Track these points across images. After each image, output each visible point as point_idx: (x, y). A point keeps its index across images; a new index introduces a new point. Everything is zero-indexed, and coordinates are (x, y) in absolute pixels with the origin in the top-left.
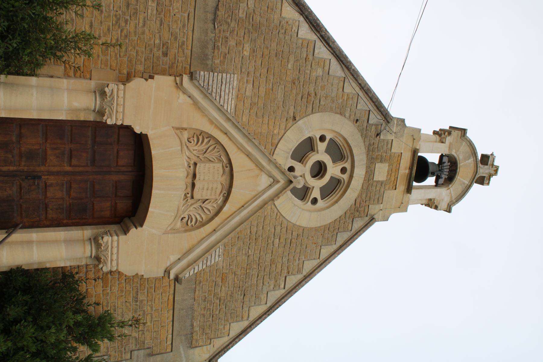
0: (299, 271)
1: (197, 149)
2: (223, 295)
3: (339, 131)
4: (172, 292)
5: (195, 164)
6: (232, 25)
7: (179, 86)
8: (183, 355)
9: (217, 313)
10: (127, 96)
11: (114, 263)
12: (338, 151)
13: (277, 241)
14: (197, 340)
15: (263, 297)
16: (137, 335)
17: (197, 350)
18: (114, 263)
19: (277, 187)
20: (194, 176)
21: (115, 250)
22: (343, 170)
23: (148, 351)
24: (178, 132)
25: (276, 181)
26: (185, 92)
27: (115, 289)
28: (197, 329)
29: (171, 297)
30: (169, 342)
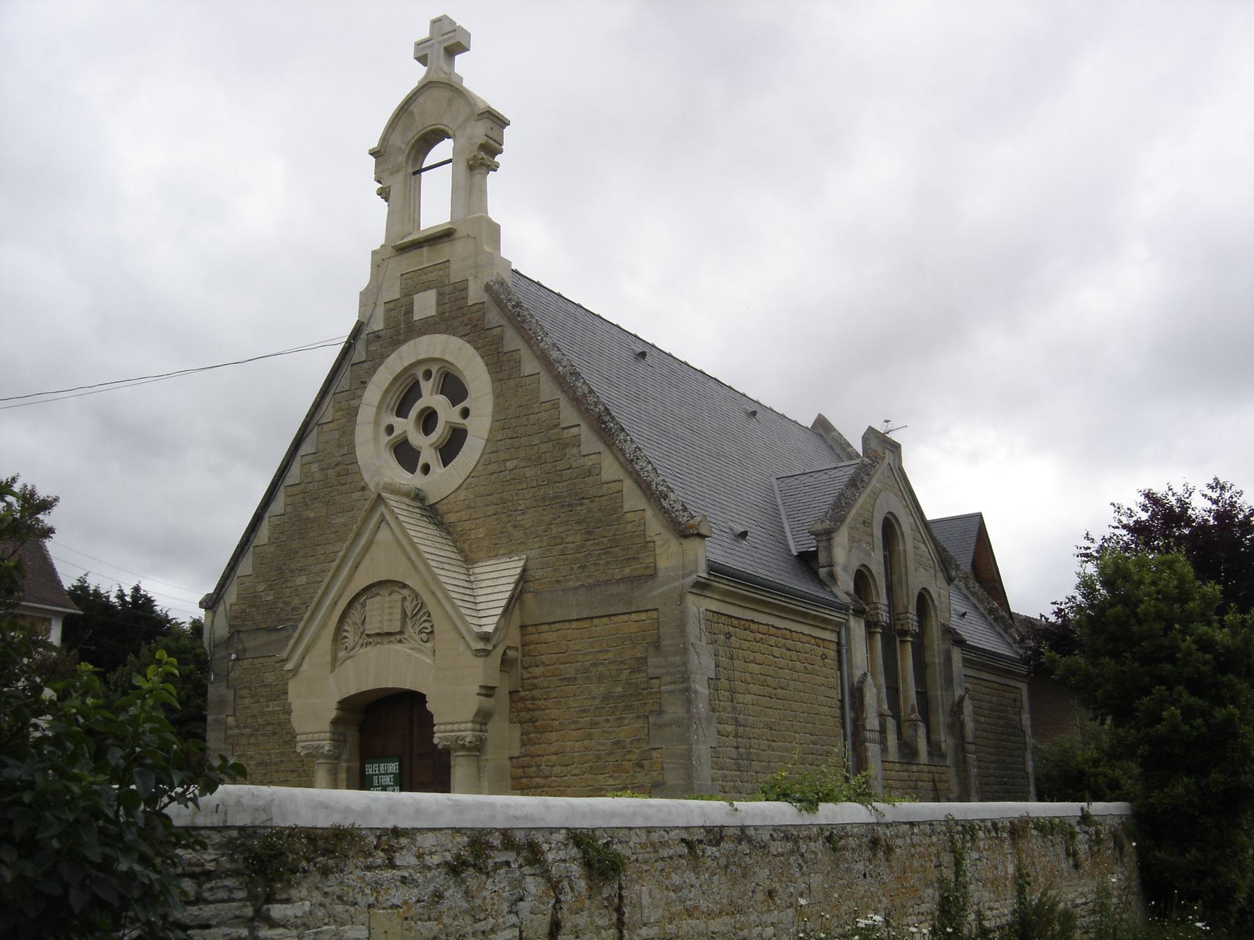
0: (556, 406)
1: (351, 636)
2: (579, 537)
3: (374, 410)
4: (566, 625)
5: (368, 636)
6: (281, 605)
7: (295, 672)
8: (666, 588)
9: (605, 540)
10: (448, 720)
11: (463, 726)
12: (404, 397)
13: (510, 465)
14: (647, 567)
15: (589, 462)
16: (626, 672)
17: (663, 564)
18: (463, 726)
19: (388, 517)
20: (378, 634)
21: (449, 727)
22: (428, 375)
23: (651, 650)
24: (338, 663)
25: (383, 519)
26: (299, 665)
27: (555, 713)
28: (627, 571)
29: (574, 625)
30: (643, 616)
